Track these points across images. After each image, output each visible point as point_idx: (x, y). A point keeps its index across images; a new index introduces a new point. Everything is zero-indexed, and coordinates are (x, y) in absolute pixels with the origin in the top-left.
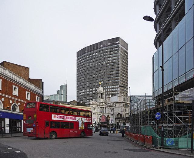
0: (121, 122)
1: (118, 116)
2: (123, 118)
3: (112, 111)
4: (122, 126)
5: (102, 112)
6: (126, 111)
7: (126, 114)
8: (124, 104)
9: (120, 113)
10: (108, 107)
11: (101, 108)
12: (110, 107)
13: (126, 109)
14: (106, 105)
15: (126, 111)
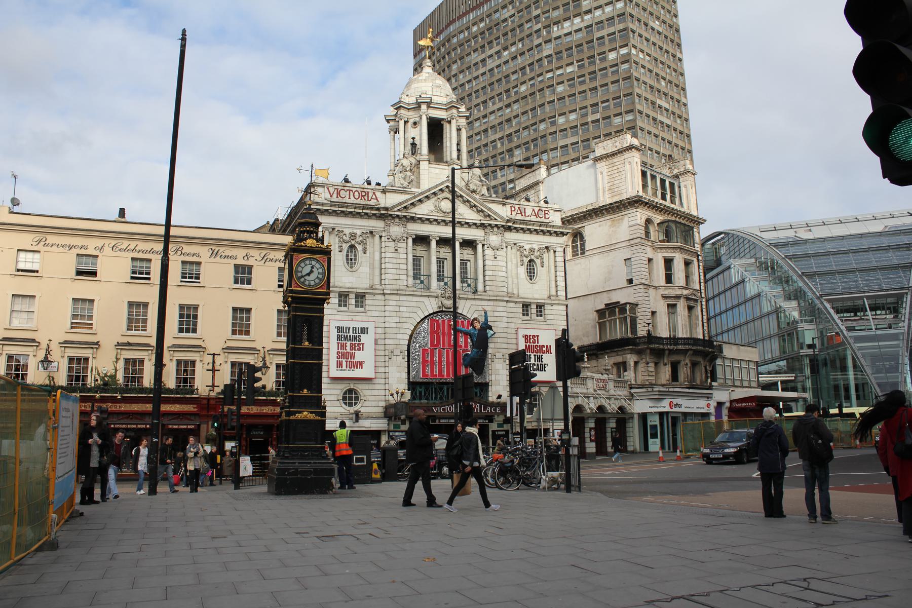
0: (629, 375)
1: (602, 326)
2: (651, 338)
3: (531, 274)
4: (644, 417)
5: (434, 283)
6: (669, 279)
7: (672, 307)
8: (648, 221)
9: (622, 297)
10: (494, 239)
11: (422, 240)
12: (511, 236)
13: (668, 262)
14: (464, 212)
15: (669, 279)
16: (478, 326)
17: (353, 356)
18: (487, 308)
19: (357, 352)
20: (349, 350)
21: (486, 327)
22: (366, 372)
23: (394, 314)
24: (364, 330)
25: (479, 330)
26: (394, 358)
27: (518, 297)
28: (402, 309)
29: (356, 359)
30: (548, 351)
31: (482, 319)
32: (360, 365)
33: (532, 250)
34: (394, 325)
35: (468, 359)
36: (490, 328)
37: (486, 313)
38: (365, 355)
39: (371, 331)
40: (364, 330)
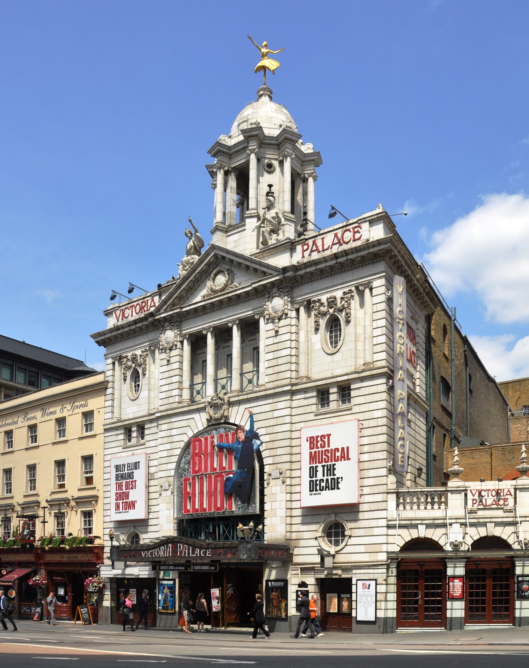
10: (278, 303)
16: (242, 436)
17: (127, 496)
18: (255, 411)
19: (131, 491)
20: (124, 490)
21: (253, 435)
22: (138, 513)
23: (165, 440)
24: (136, 465)
25: (243, 442)
26: (164, 493)
27: (309, 379)
28: (174, 432)
29: (131, 499)
30: (345, 455)
31: (247, 428)
32: (131, 505)
33: (332, 302)
34: (165, 454)
35: (230, 484)
36: (257, 437)
37: (251, 416)
38: (137, 495)
39: (142, 465)
40: (136, 465)
